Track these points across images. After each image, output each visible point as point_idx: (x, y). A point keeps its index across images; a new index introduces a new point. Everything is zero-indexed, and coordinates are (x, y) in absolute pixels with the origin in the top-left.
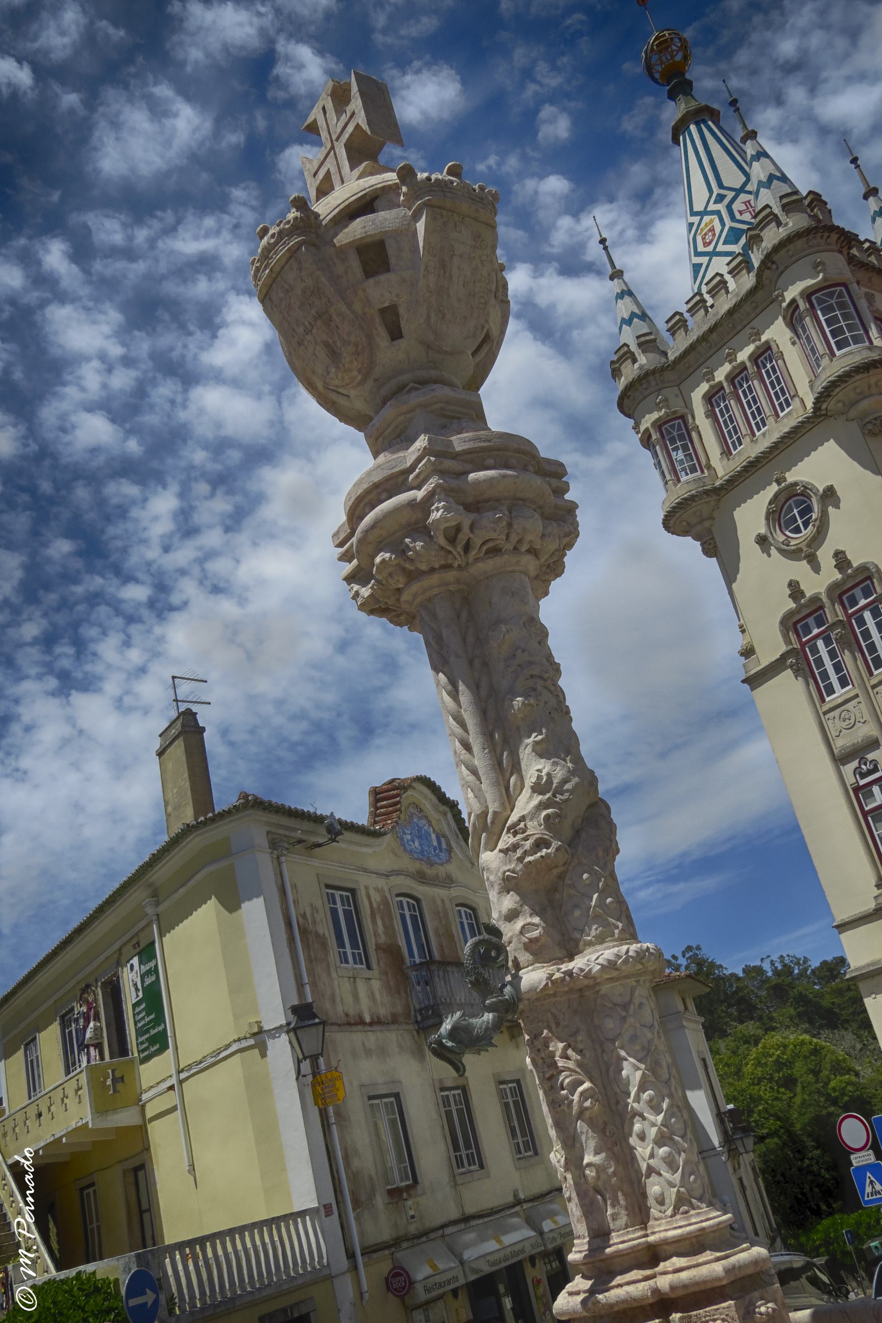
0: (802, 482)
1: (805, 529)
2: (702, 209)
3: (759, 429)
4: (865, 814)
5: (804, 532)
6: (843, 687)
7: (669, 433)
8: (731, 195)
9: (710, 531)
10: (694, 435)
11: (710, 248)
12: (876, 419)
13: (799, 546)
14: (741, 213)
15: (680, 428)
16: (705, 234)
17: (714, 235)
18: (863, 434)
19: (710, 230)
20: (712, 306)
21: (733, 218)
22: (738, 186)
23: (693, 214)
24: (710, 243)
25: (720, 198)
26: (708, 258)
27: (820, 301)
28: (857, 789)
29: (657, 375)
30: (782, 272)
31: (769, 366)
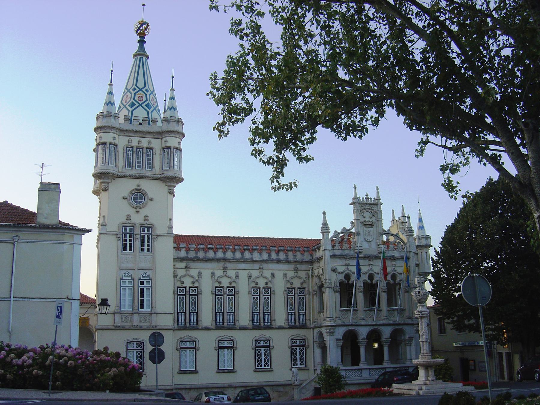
3: (138, 168)
4: (121, 286)
5: (138, 204)
6: (129, 251)
7: (111, 148)
8: (150, 92)
9: (108, 183)
11: (140, 103)
19: (141, 97)
20: (140, 124)
22: (152, 91)
23: (136, 85)
24: (140, 101)
25: (147, 90)
26: (138, 105)
28: (121, 279)
30: (171, 136)
31: (149, 153)
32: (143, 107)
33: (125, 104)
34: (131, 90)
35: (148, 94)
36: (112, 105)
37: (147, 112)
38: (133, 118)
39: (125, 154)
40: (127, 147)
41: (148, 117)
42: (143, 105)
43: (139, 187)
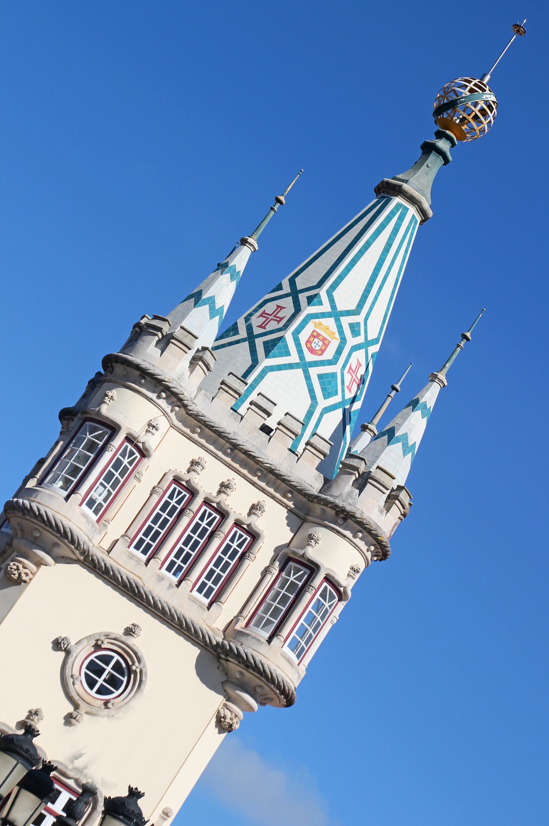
0: (145, 666)
1: (98, 692)
2: (340, 307)
3: (169, 569)
5: (93, 692)
10: (132, 482)
11: (309, 357)
12: (236, 716)
13: (80, 702)
14: (350, 368)
15: (130, 463)
16: (319, 335)
17: (323, 351)
18: (218, 712)
19: (324, 339)
21: (344, 367)
22: (370, 338)
23: (330, 293)
24: (312, 351)
25: (355, 329)
27: (323, 595)
29: (179, 404)
32: (308, 378)
33: (257, 331)
34: (302, 297)
35: (352, 341)
36: (212, 316)
37: (309, 402)
38: (253, 396)
39: (156, 498)
40: (176, 480)
41: (304, 425)
42: (314, 372)
43: (131, 641)
